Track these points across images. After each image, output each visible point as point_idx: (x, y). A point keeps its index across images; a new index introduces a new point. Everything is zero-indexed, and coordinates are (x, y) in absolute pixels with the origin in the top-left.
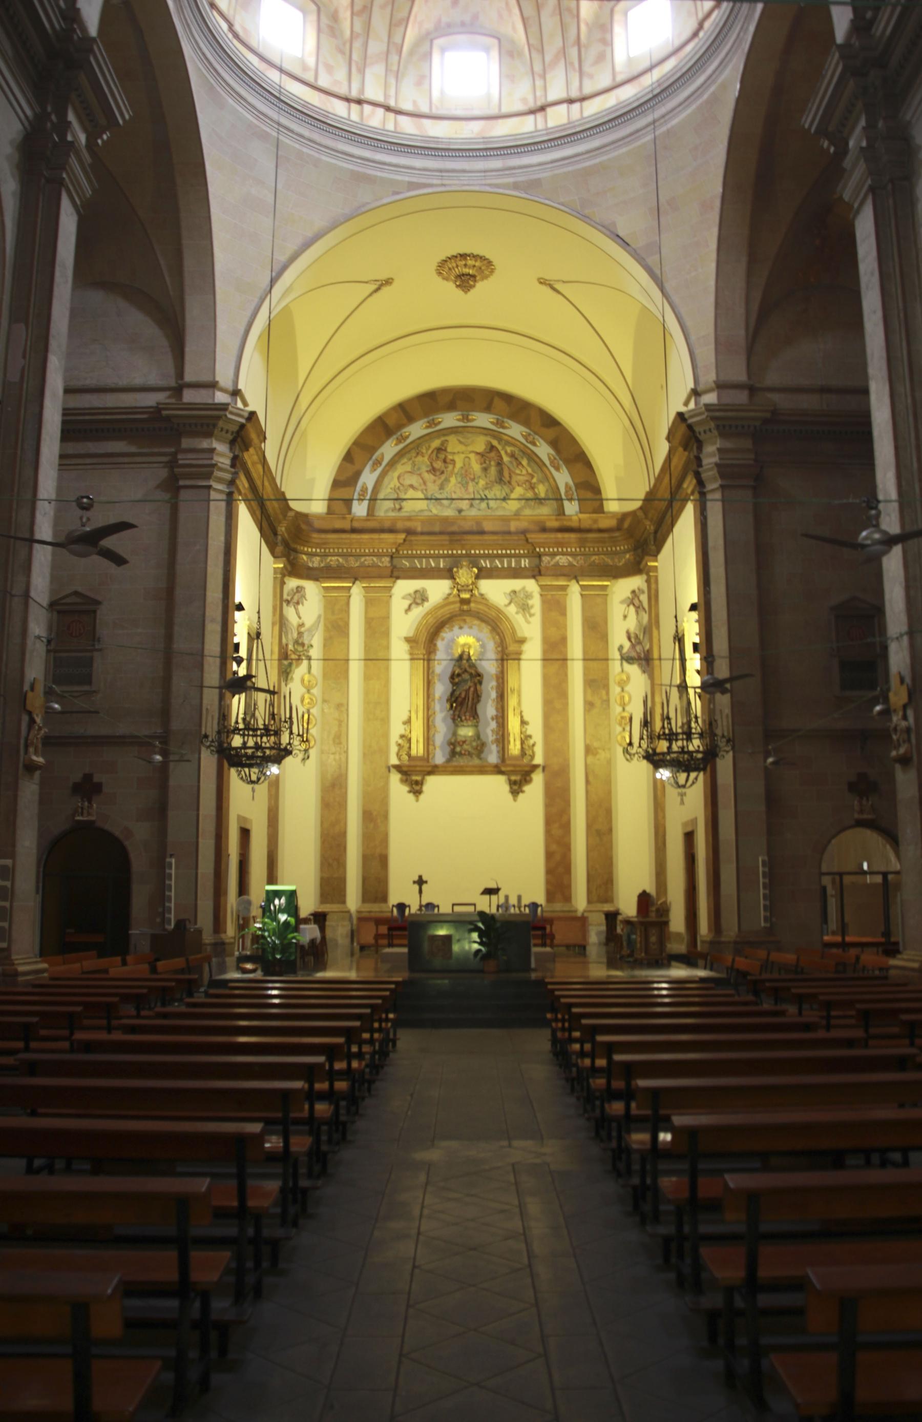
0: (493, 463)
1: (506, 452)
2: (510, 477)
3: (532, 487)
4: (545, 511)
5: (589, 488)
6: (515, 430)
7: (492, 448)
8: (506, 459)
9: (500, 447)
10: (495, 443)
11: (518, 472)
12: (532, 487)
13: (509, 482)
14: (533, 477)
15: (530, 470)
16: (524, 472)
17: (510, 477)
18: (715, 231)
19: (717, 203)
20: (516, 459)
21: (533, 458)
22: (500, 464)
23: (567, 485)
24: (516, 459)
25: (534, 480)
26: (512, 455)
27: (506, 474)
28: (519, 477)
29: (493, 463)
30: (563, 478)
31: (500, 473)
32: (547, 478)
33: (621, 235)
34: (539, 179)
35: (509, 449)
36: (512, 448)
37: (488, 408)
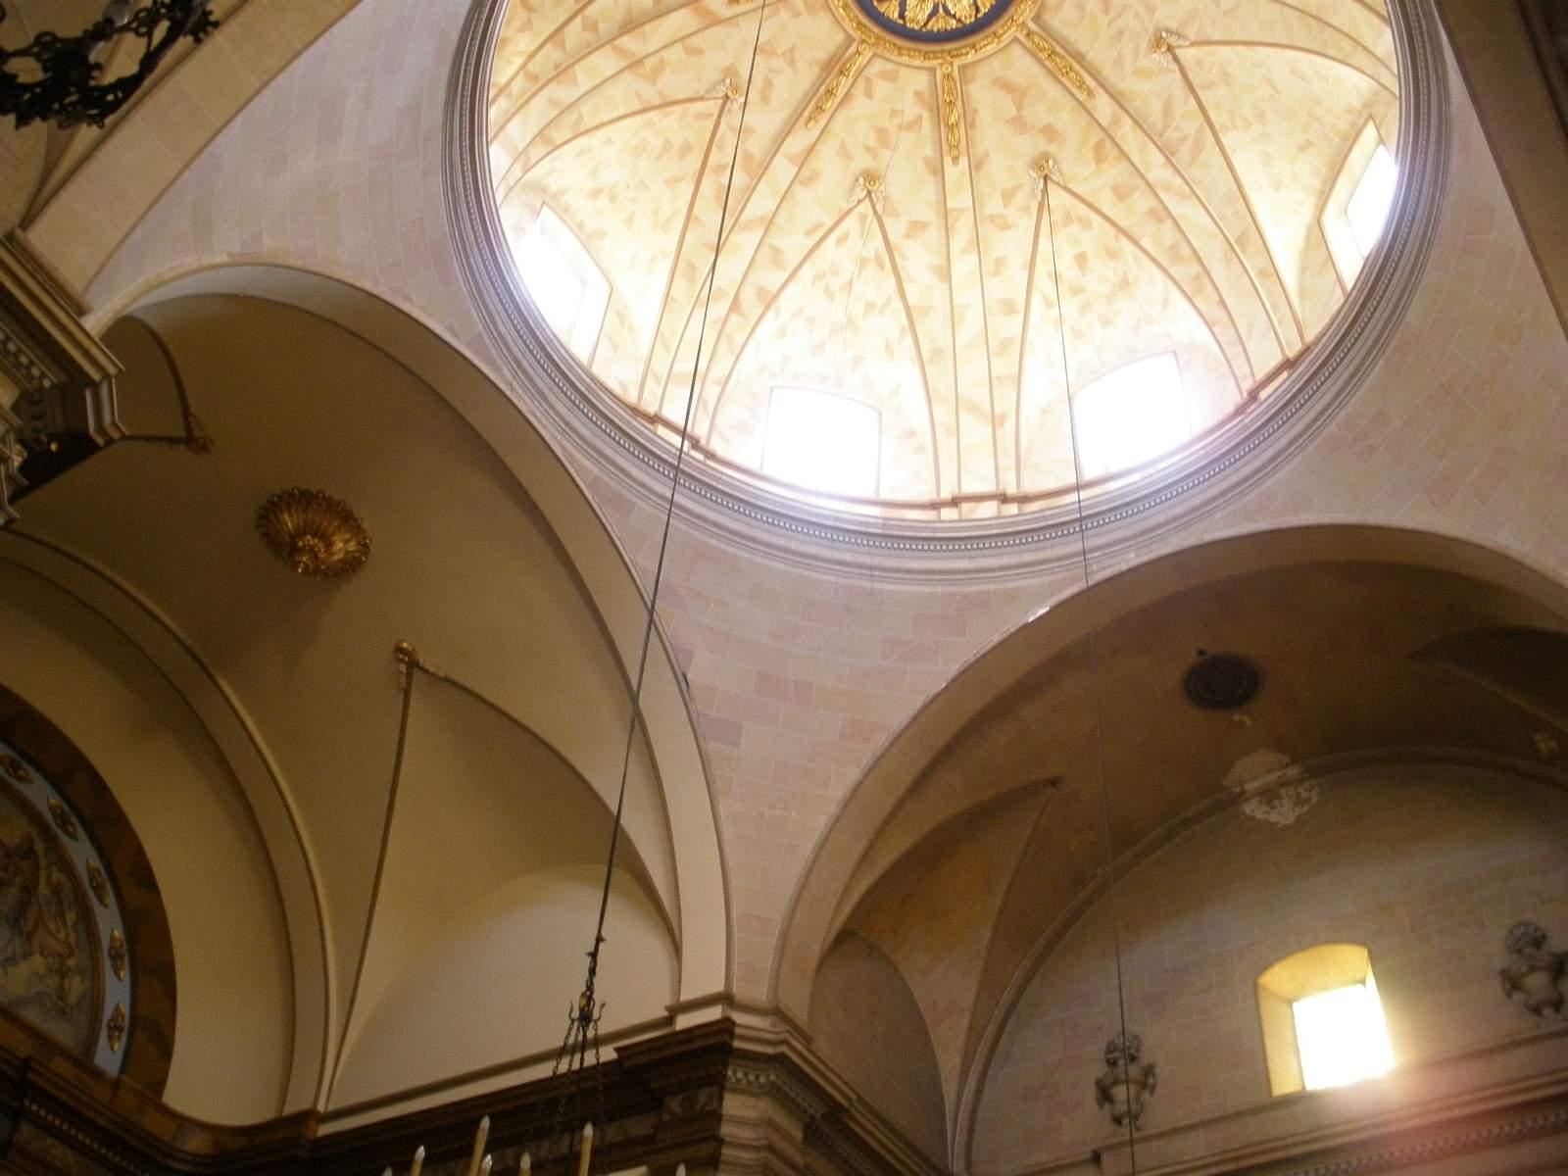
0: (18, 880)
1: (49, 876)
2: (35, 927)
3: (62, 973)
4: (64, 1033)
5: (153, 1033)
6: (82, 853)
7: (30, 853)
8: (43, 890)
9: (43, 861)
10: (39, 846)
11: (52, 926)
12: (62, 973)
13: (29, 937)
14: (71, 954)
15: (72, 939)
16: (61, 936)
17: (35, 927)
18: (853, 774)
19: (881, 740)
20: (60, 902)
21: (87, 918)
22: (29, 890)
23: (117, 1009)
24: (60, 902)
25: (71, 962)
26: (56, 890)
27: (31, 916)
28: (53, 942)
29: (18, 880)
30: (117, 993)
31: (22, 909)
32: (94, 973)
33: (689, 677)
34: (634, 504)
35: (56, 875)
36: (63, 879)
37: (57, 783)
